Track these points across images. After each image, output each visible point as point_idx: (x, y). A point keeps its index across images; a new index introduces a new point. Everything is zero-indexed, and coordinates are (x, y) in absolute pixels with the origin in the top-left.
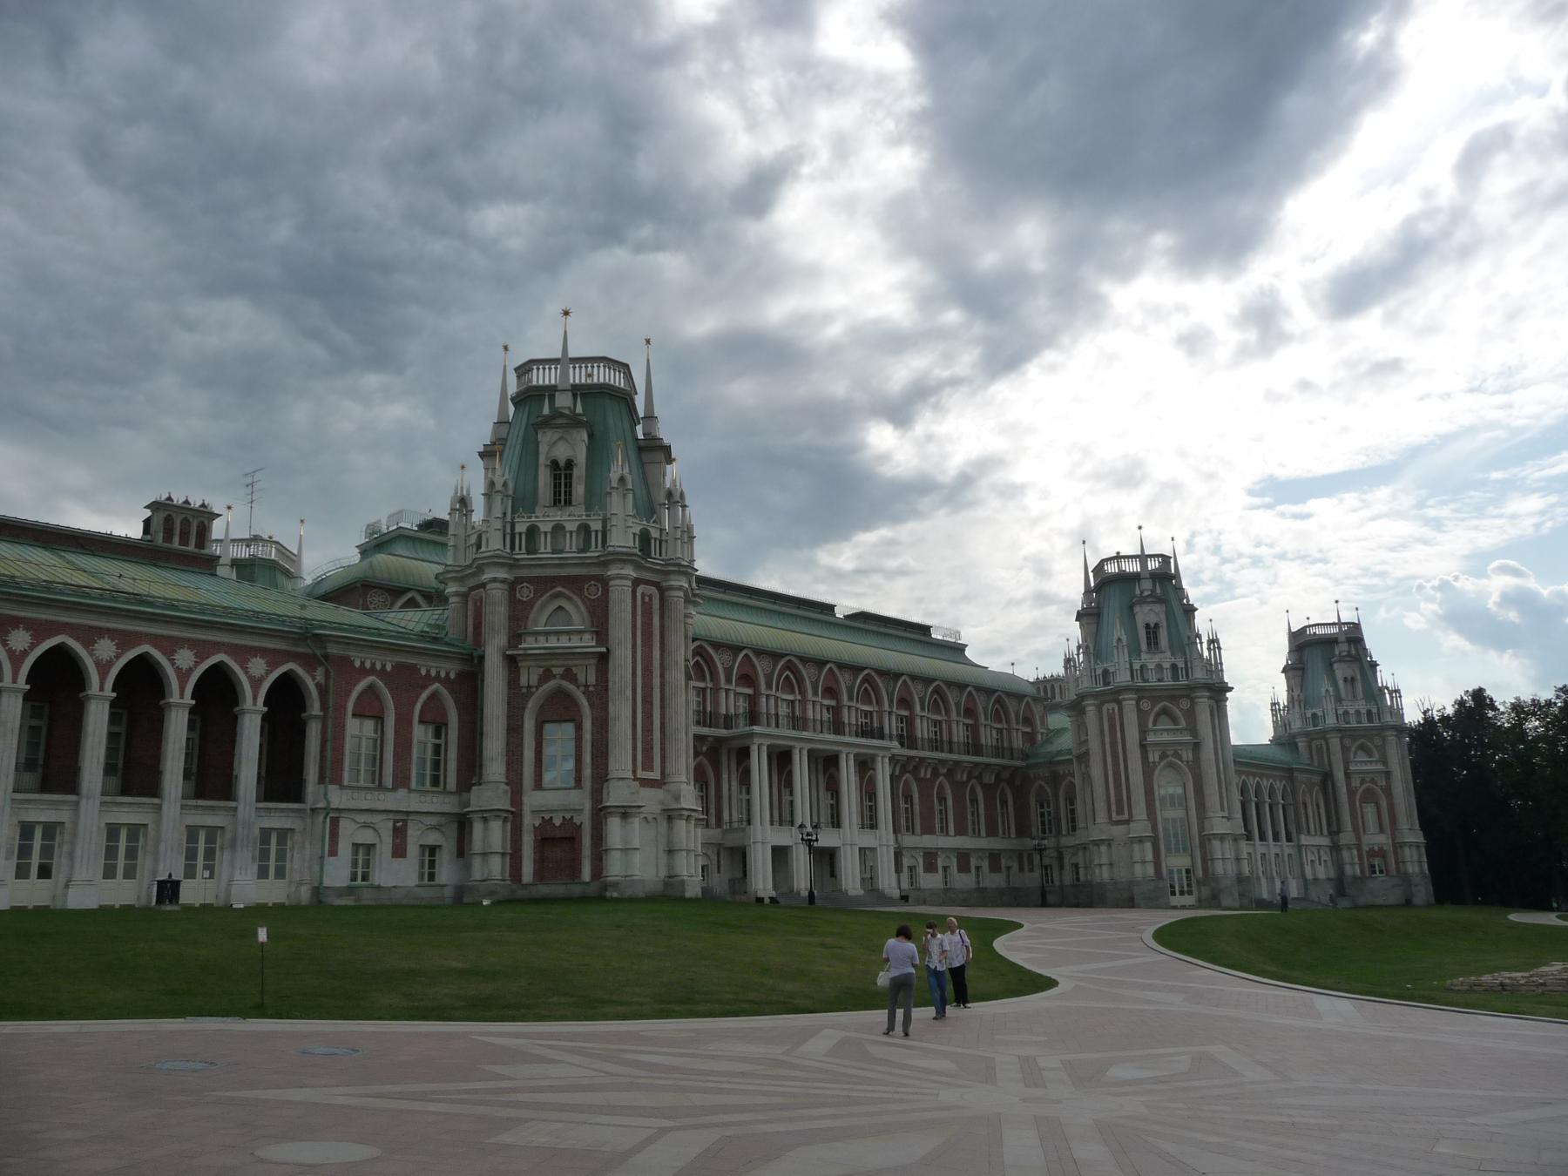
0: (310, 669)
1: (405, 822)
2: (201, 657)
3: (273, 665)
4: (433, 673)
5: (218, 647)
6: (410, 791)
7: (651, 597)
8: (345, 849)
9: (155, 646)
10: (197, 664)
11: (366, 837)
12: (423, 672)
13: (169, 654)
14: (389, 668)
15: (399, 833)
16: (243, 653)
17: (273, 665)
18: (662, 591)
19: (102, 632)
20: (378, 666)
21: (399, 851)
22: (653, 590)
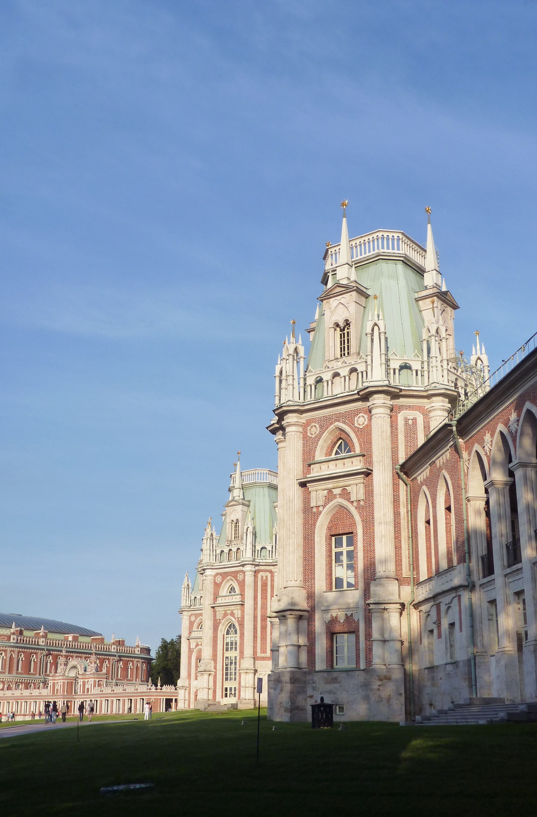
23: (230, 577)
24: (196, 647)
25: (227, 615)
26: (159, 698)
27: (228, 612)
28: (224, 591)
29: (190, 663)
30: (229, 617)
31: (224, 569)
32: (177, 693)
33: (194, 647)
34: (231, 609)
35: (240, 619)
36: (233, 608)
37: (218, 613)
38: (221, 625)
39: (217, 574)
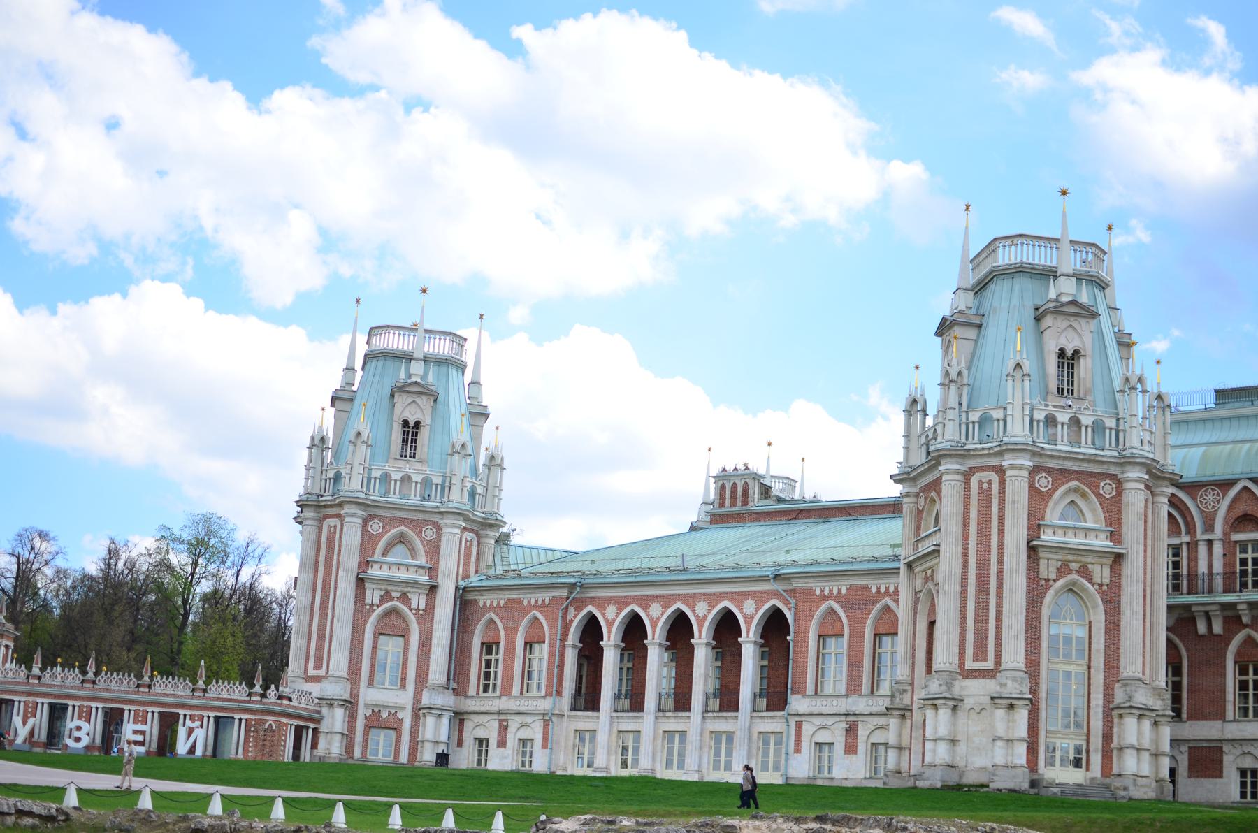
0: (787, 603)
1: (856, 723)
2: (712, 606)
3: (759, 604)
4: (883, 590)
5: (722, 596)
6: (861, 696)
7: (990, 483)
8: (806, 745)
9: (684, 603)
10: (710, 611)
11: (823, 737)
12: (874, 590)
13: (692, 607)
14: (844, 591)
15: (851, 731)
16: (739, 597)
17: (759, 604)
18: (1000, 471)
19: (653, 598)
20: (835, 591)
21: (851, 749)
22: (994, 477)
23: (1075, 483)
24: (382, 601)
25: (1070, 571)
26: (285, 720)
27: (1074, 566)
28: (1053, 515)
29: (356, 642)
30: (1074, 576)
31: (1060, 462)
32: (319, 712)
33: (376, 601)
34: (1084, 559)
35: (1105, 588)
36: (1089, 560)
37: (1043, 563)
38: (1051, 592)
39: (1035, 470)
